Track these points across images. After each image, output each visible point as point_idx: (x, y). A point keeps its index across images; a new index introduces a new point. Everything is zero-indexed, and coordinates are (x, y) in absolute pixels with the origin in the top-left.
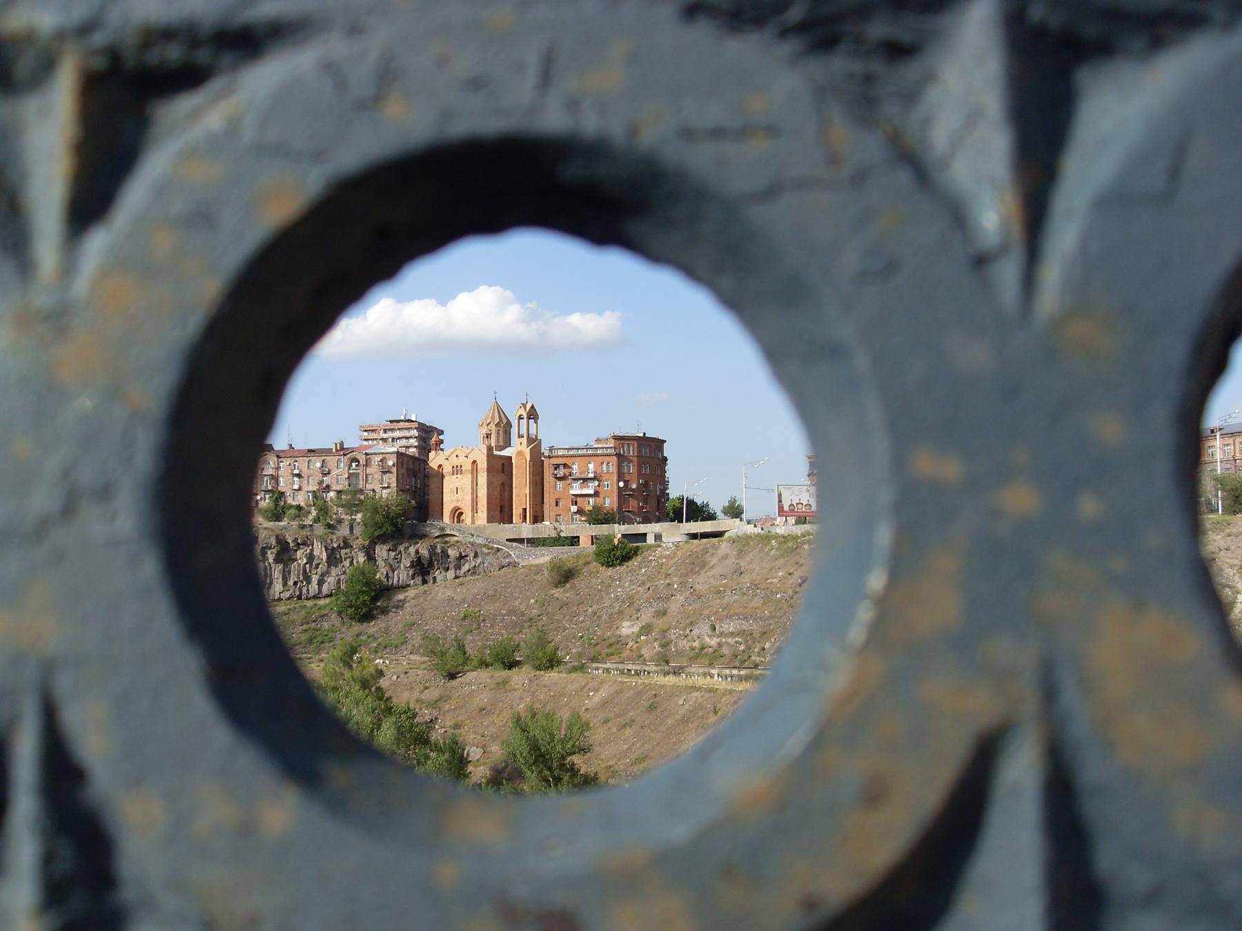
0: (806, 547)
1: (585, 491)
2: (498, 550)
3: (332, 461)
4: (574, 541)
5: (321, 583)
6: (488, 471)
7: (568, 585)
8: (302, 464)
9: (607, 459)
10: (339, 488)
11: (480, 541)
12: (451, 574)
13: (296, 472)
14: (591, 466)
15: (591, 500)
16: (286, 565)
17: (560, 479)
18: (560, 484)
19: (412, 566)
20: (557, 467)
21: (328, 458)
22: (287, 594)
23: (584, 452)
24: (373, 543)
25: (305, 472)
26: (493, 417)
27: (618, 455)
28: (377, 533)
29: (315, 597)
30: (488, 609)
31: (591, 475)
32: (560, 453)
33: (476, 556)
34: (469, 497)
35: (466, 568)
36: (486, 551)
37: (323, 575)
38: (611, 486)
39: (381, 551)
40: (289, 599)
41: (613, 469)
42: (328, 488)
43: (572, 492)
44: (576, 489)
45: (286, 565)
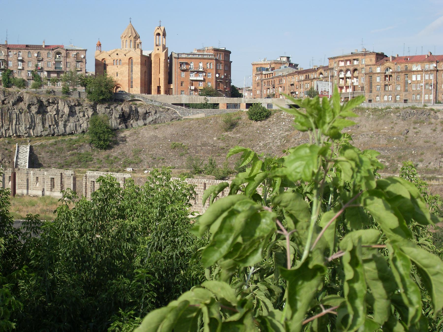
0: (392, 114)
1: (199, 78)
2: (168, 109)
3: (44, 53)
4: (215, 106)
5: (65, 126)
6: (141, 65)
7: (234, 130)
8: (23, 54)
9: (210, 61)
10: (48, 70)
11: (157, 104)
12: (141, 122)
13: (20, 58)
14: (201, 65)
15: (201, 83)
16: (43, 115)
17: (184, 71)
18: (183, 74)
19: (119, 118)
20: (181, 64)
21: (41, 51)
22: (46, 133)
23: (190, 56)
24: (96, 104)
25: (26, 59)
26: (132, 33)
27: (216, 59)
28: (101, 98)
29: (63, 135)
30: (185, 142)
31: (201, 70)
32: (184, 56)
33: (156, 113)
34: (127, 78)
35: (150, 119)
36: (161, 110)
37: (66, 122)
38: (212, 77)
39: (101, 108)
40: (47, 135)
41: (213, 66)
42: (42, 70)
43: (191, 78)
44: (193, 77)
45: (43, 115)
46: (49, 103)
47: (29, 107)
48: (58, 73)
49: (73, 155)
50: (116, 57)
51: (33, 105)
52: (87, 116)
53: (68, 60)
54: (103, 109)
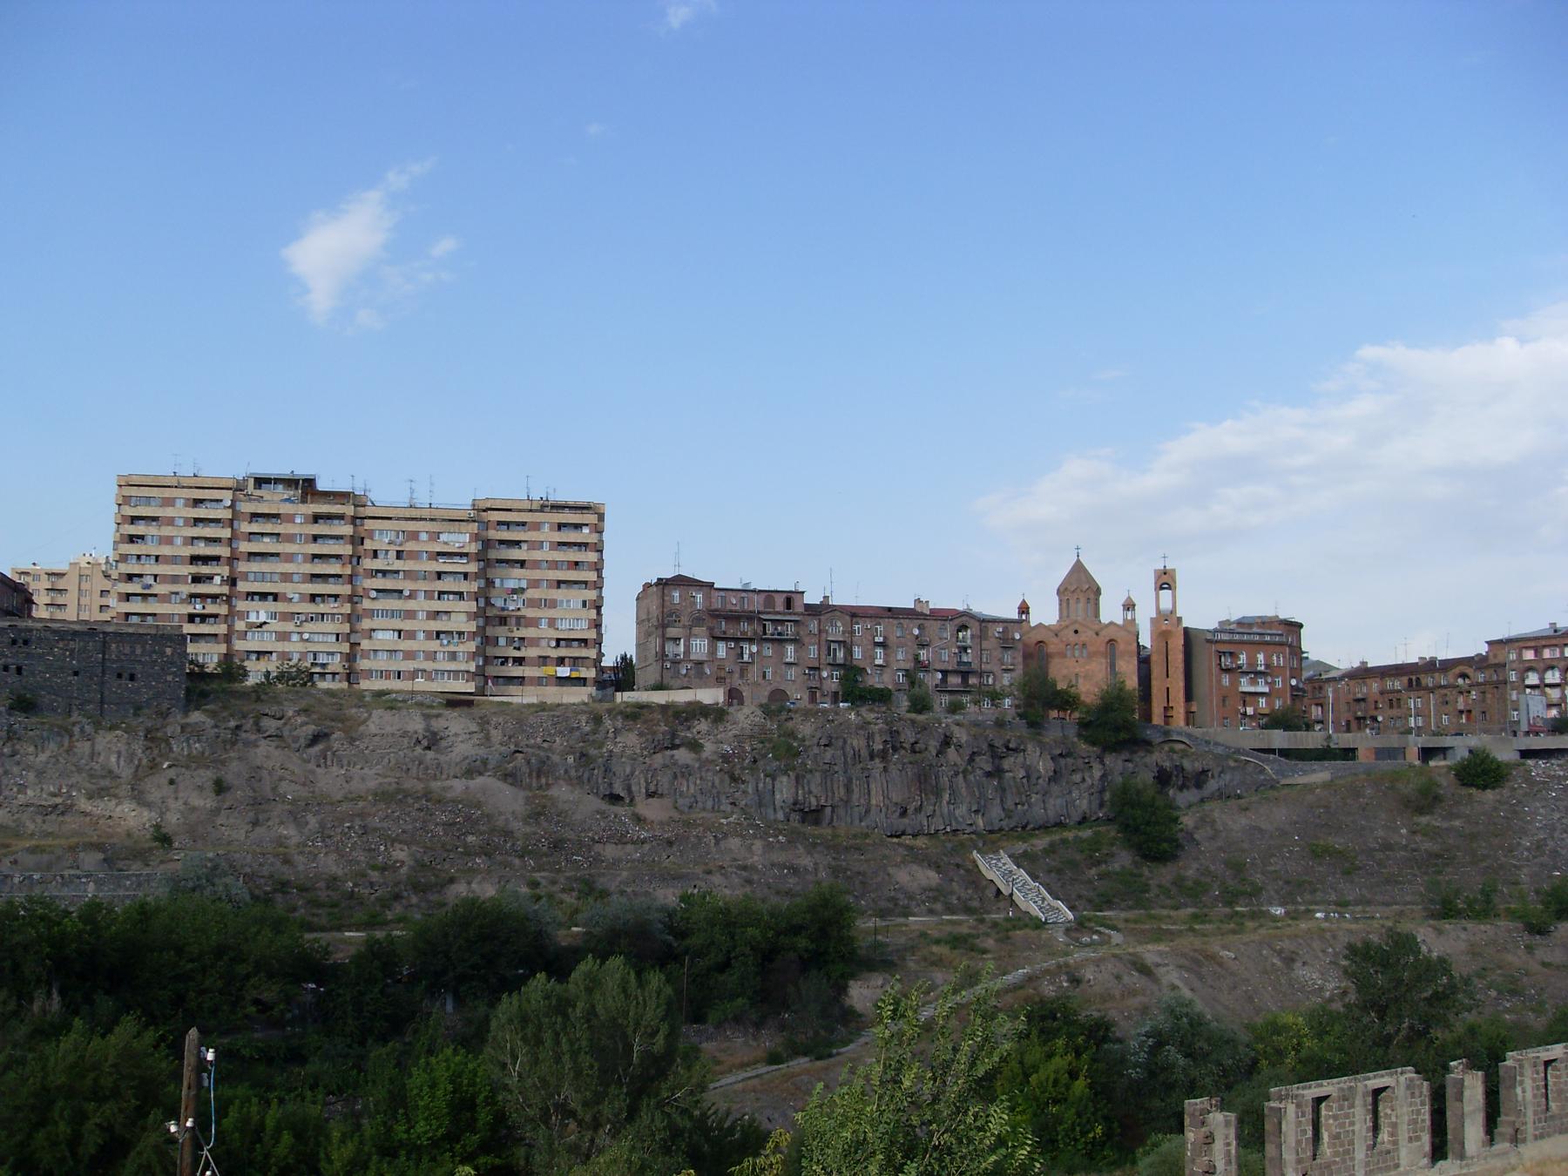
3: (933, 626)
11: (1219, 750)
13: (879, 639)
17: (1227, 670)
18: (1226, 680)
20: (1220, 654)
21: (927, 623)
36: (1232, 764)
44: (1245, 686)
46: (1008, 749)
47: (971, 760)
48: (965, 675)
49: (1101, 876)
50: (1072, 638)
51: (979, 754)
52: (1089, 781)
53: (985, 644)
54: (1120, 762)
